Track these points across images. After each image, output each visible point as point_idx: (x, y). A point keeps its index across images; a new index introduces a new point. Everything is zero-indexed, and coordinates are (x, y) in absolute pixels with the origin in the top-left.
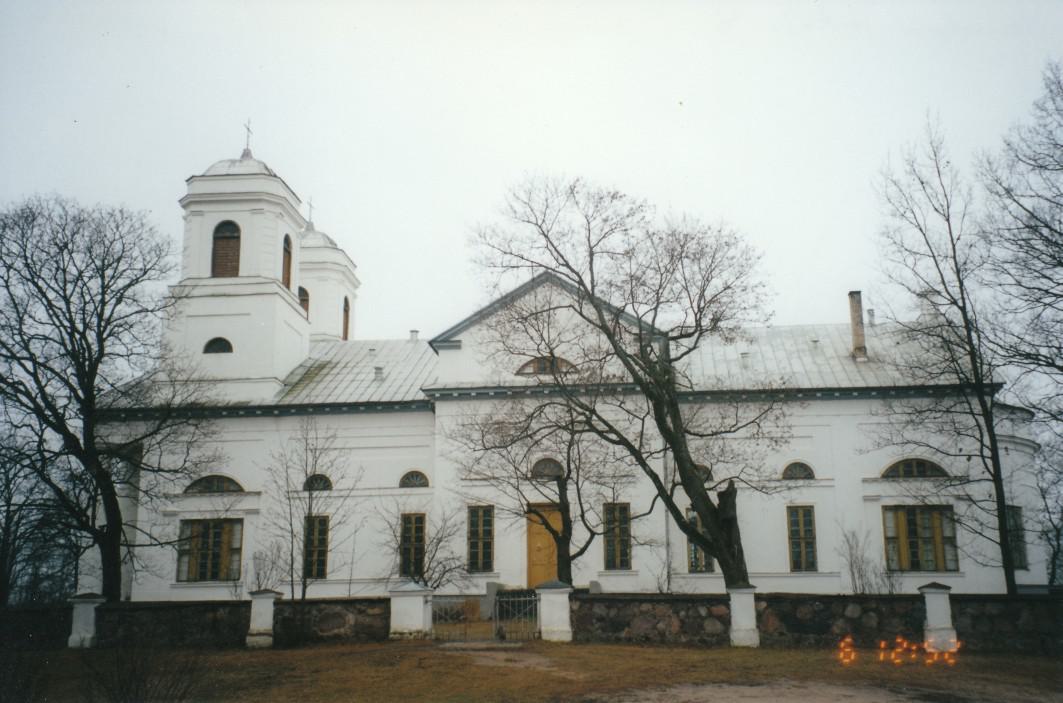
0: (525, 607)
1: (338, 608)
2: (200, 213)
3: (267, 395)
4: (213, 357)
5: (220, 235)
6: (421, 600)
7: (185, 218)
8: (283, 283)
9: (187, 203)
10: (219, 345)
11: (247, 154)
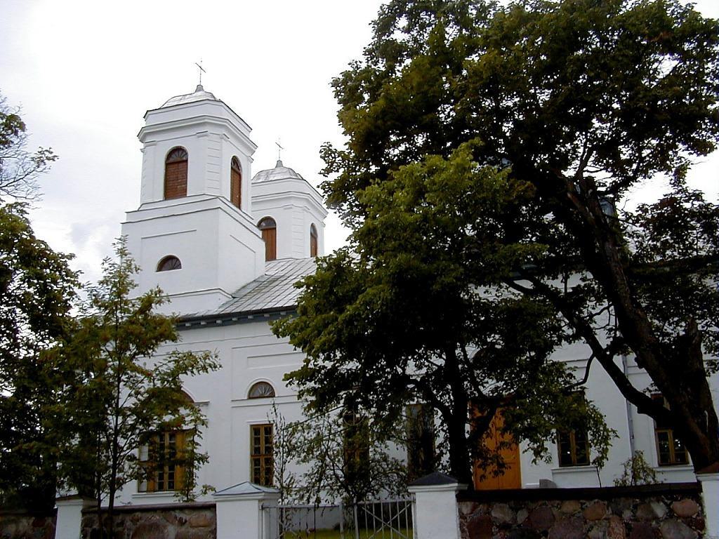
0: (394, 513)
1: (156, 517)
2: (153, 143)
3: (212, 306)
4: (165, 274)
5: (171, 160)
6: (254, 506)
7: (142, 151)
8: (232, 201)
9: (143, 136)
10: (169, 263)
11: (199, 88)
